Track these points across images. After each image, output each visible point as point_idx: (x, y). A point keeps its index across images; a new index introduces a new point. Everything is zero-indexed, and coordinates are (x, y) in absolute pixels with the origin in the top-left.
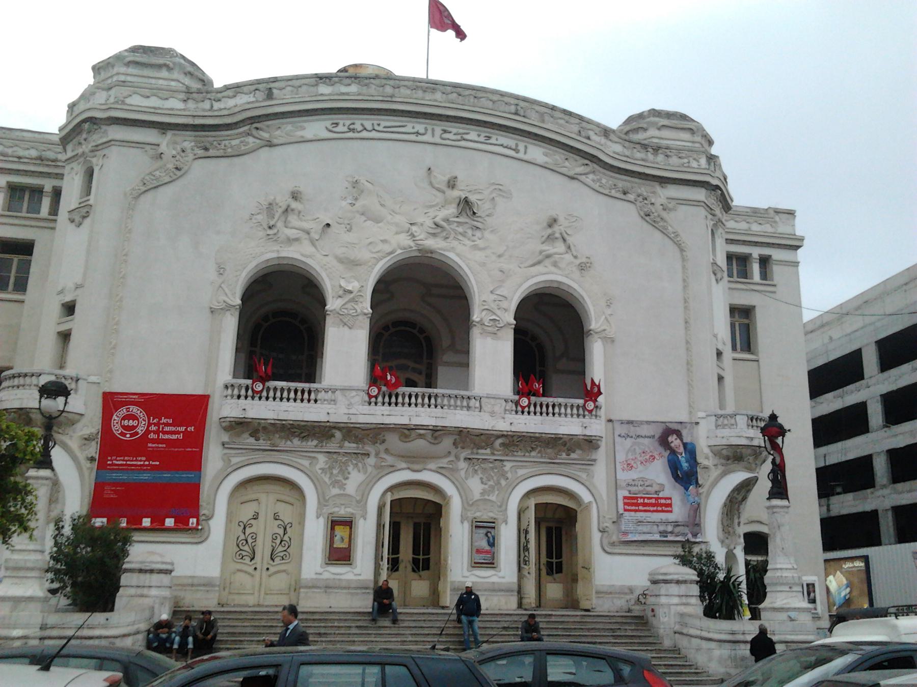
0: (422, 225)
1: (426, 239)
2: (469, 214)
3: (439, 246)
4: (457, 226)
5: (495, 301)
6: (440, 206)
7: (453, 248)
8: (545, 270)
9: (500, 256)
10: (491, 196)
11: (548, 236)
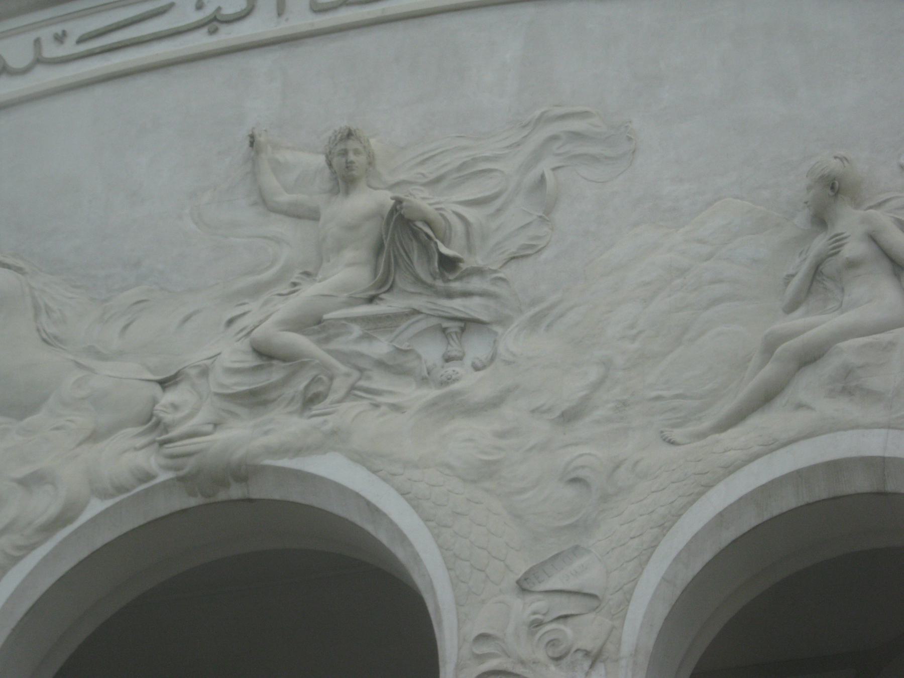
0: (205, 372)
1: (216, 425)
2: (422, 271)
3: (273, 440)
4: (366, 337)
5: (538, 624)
6: (295, 276)
7: (334, 433)
8: (799, 420)
9: (570, 416)
10: (533, 175)
11: (816, 271)
